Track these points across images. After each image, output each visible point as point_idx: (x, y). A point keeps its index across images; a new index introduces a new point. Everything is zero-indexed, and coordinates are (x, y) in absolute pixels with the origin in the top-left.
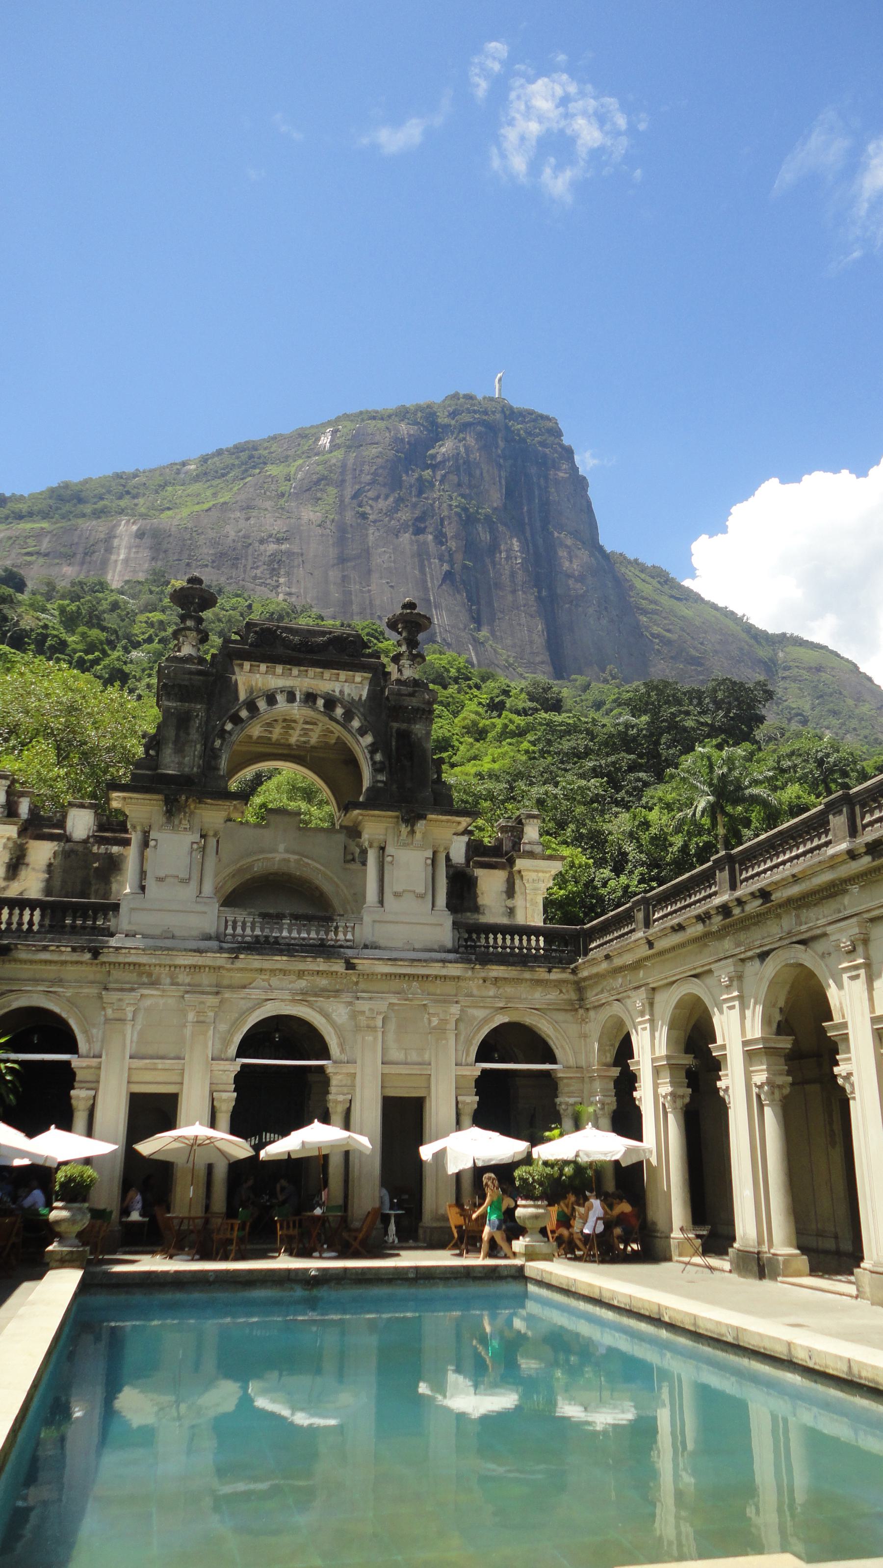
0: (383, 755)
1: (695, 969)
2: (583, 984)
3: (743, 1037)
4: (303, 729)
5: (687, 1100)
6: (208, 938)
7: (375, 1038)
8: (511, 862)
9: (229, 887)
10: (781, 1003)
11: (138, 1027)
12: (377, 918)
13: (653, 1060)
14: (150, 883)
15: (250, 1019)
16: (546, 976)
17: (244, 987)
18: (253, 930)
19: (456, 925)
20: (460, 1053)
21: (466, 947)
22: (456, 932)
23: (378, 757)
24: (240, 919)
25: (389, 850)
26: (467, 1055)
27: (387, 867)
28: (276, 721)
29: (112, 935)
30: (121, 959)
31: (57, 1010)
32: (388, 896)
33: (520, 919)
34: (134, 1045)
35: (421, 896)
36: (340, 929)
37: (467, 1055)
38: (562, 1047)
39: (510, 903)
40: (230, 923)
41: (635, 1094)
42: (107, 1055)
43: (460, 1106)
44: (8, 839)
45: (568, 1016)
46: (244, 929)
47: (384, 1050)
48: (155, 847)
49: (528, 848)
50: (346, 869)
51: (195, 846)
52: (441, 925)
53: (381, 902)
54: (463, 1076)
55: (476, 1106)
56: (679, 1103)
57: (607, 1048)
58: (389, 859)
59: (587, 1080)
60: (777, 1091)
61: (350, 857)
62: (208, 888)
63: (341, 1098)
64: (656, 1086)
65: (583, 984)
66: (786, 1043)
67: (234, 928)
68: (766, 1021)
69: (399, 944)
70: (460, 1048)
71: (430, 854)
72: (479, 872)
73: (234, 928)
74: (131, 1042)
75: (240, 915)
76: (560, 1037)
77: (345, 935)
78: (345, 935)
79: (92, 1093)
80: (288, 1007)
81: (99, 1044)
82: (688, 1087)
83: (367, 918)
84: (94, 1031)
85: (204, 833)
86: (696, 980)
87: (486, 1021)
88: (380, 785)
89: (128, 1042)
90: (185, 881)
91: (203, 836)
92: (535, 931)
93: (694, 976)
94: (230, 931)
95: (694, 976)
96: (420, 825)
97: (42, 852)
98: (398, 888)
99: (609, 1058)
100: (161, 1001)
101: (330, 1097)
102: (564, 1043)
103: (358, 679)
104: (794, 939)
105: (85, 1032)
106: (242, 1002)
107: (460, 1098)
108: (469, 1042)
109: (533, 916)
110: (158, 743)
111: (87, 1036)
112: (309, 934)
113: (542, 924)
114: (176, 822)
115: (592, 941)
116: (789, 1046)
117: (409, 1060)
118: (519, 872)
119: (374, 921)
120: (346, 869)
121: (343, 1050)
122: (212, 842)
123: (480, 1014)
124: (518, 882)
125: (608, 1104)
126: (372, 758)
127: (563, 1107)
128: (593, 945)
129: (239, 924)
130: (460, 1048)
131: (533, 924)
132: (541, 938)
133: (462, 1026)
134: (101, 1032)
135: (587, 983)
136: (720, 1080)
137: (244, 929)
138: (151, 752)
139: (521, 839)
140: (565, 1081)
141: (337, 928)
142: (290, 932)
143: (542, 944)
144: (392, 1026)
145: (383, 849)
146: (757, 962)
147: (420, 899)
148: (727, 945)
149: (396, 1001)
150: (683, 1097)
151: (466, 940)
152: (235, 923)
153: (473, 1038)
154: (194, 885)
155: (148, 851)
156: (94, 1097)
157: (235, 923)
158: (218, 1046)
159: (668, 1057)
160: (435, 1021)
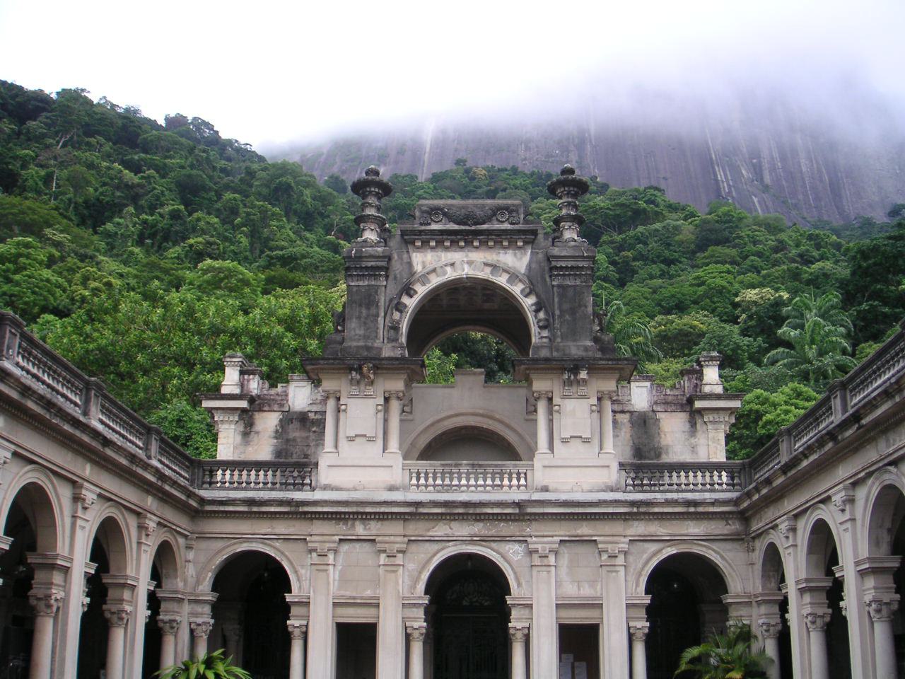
0: (547, 313)
1: (820, 495)
2: (747, 515)
3: (855, 558)
4: (484, 295)
5: (828, 619)
6: (392, 488)
7: (549, 572)
8: (690, 401)
9: (423, 442)
10: (888, 524)
11: (340, 568)
12: (547, 464)
13: (797, 582)
14: (343, 443)
15: (436, 558)
16: (711, 509)
17: (428, 530)
18: (435, 480)
19: (621, 465)
20: (630, 584)
21: (634, 486)
22: (623, 472)
23: (542, 315)
24: (422, 470)
25: (556, 400)
26: (637, 585)
27: (556, 416)
28: (456, 289)
29: (313, 490)
30: (319, 509)
31: (273, 555)
32: (557, 442)
33: (702, 457)
34: (336, 583)
35: (587, 441)
36: (514, 476)
37: (637, 585)
38: (729, 574)
39: (693, 440)
40: (414, 475)
41: (786, 615)
42: (314, 591)
43: (631, 631)
44: (243, 411)
45: (736, 545)
46: (426, 479)
47: (559, 584)
48: (345, 411)
49: (707, 389)
50: (527, 420)
51: (380, 408)
52: (608, 467)
53: (551, 447)
54: (634, 605)
55: (647, 631)
56: (819, 622)
57: (771, 574)
58: (556, 408)
59: (754, 603)
60: (884, 607)
61: (533, 408)
62: (394, 444)
63: (519, 625)
64: (800, 607)
65: (747, 515)
66: (895, 563)
67: (418, 479)
68: (875, 542)
69: (568, 487)
70: (631, 578)
71: (594, 401)
72: (659, 415)
73: (418, 479)
74: (334, 580)
75: (424, 465)
76: (726, 565)
77: (519, 480)
78: (519, 480)
79: (305, 623)
80: (468, 547)
81: (308, 582)
82: (829, 607)
83: (538, 462)
84: (302, 572)
85: (387, 395)
86: (821, 506)
87: (654, 554)
88: (544, 340)
89: (332, 582)
90: (371, 440)
91: (387, 400)
92: (718, 467)
93: (822, 502)
94: (414, 481)
95: (822, 502)
96: (583, 375)
97: (268, 422)
98: (566, 435)
99: (773, 585)
100: (358, 545)
101: (510, 625)
102: (731, 571)
103: (520, 244)
104: (886, 461)
105: (296, 572)
106: (427, 544)
107: (631, 624)
108: (640, 575)
109: (715, 453)
110: (344, 320)
111: (298, 576)
112: (485, 480)
113: (725, 460)
114: (362, 387)
115: (756, 474)
116: (897, 565)
117: (582, 592)
118: (701, 412)
119: (544, 467)
120: (527, 420)
121: (519, 585)
122: (395, 406)
123: (653, 547)
124: (699, 422)
125: (773, 625)
126: (536, 317)
127: (732, 629)
128: (756, 477)
129: (422, 475)
130: (629, 578)
131: (715, 460)
132: (724, 474)
133: (631, 559)
134: (309, 572)
135: (750, 513)
136: (843, 600)
137: (426, 479)
138: (339, 328)
139: (702, 380)
140: (733, 606)
141: (510, 474)
142: (468, 480)
143: (725, 479)
144: (565, 560)
145: (550, 400)
146: (550, 488)
147: (586, 445)
148: (844, 471)
149: (567, 538)
150: (822, 617)
151: (633, 479)
152: (418, 474)
153: (642, 569)
154: (380, 442)
155: (342, 415)
156: (307, 626)
157: (418, 474)
158: (408, 582)
159: (807, 580)
160: (605, 557)
